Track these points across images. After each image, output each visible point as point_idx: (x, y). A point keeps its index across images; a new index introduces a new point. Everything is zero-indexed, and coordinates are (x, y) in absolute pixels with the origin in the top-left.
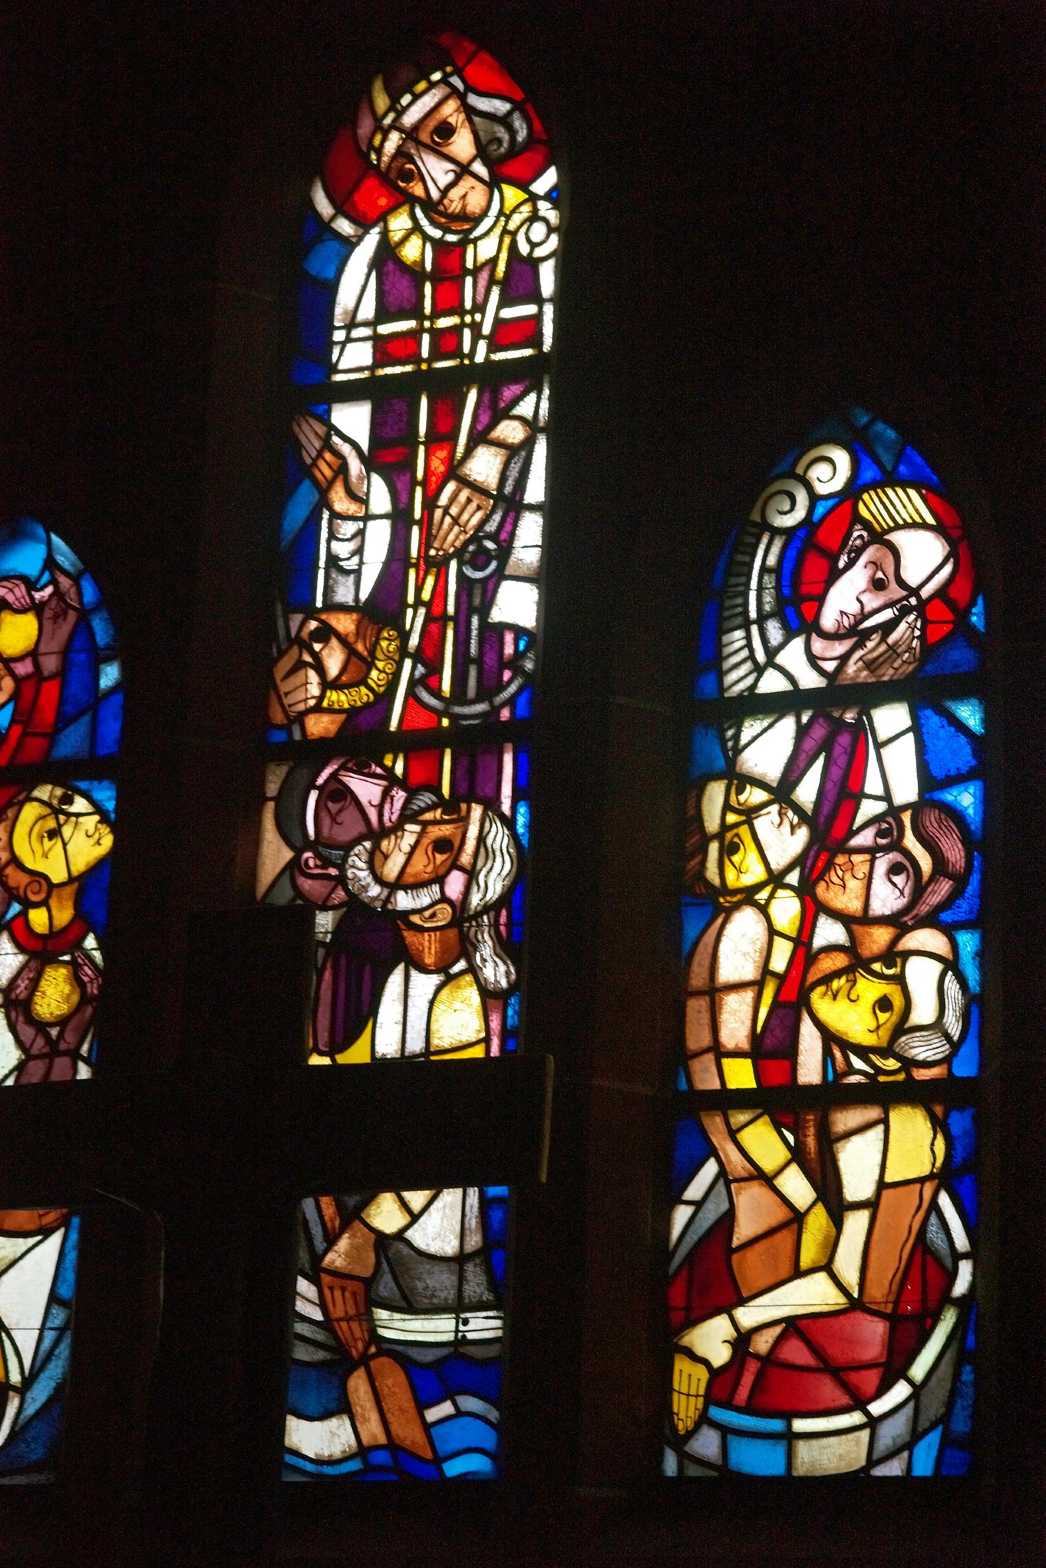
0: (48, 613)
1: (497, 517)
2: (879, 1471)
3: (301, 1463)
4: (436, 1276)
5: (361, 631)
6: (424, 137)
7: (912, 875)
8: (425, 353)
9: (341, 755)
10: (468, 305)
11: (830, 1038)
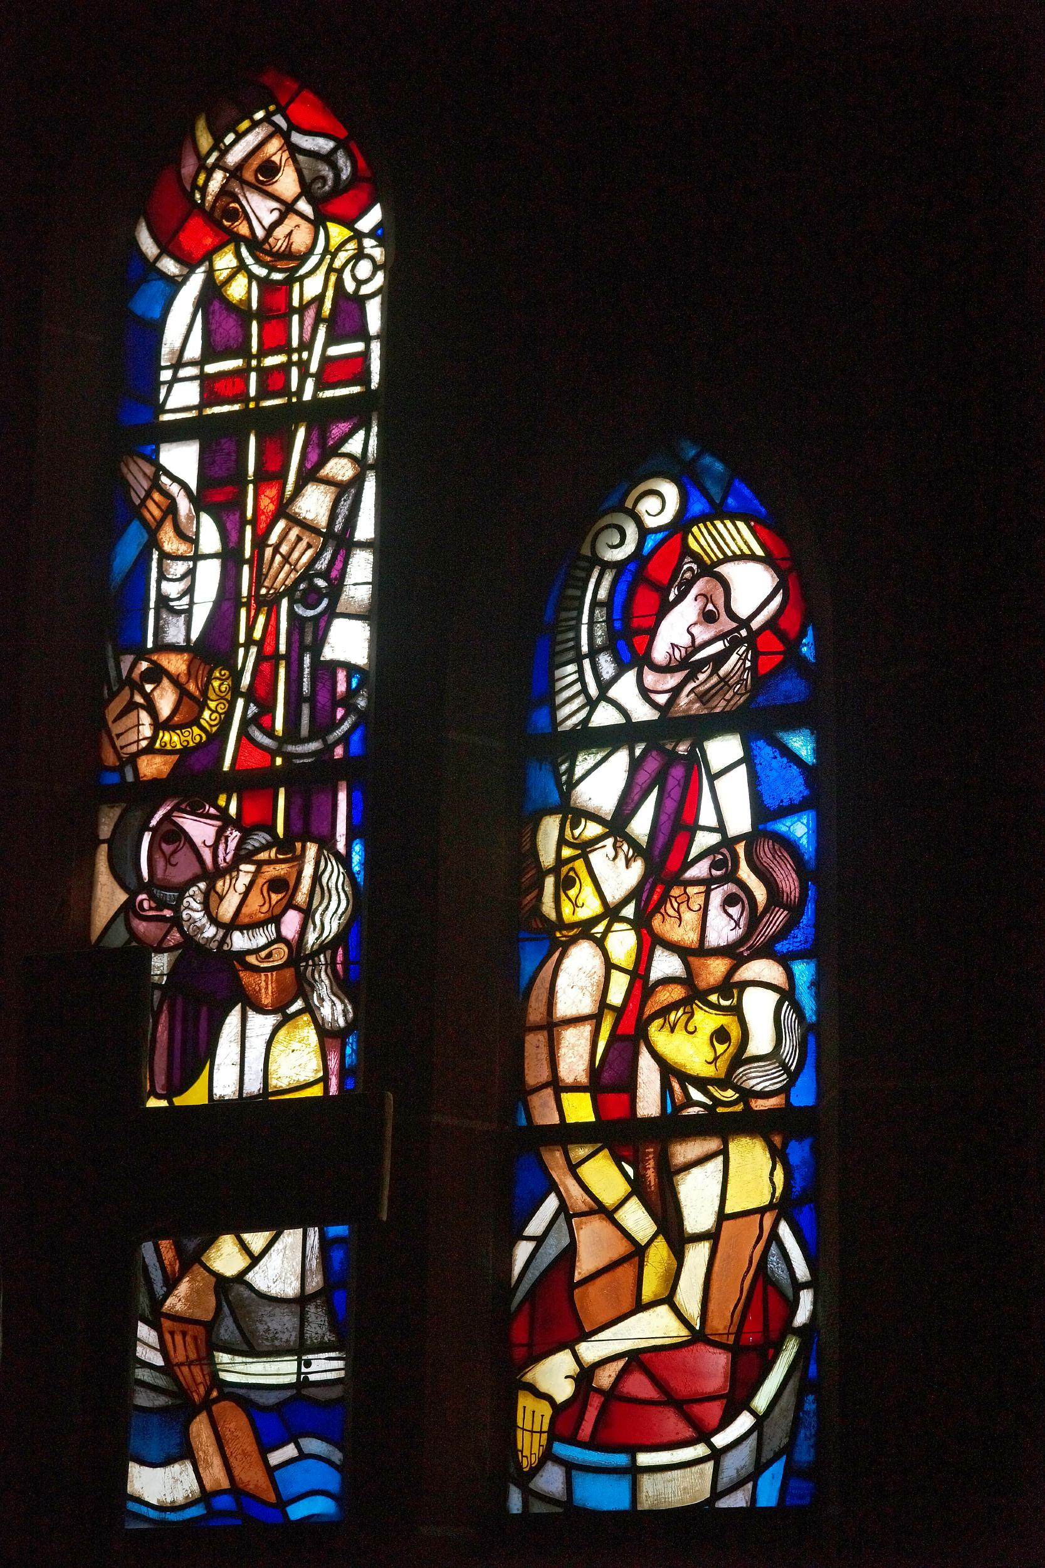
1: (328, 555)
2: (724, 1503)
3: (144, 1510)
5: (193, 672)
6: (248, 175)
7: (747, 906)
8: (252, 392)
9: (174, 796)
10: (295, 343)
11: (668, 1070)
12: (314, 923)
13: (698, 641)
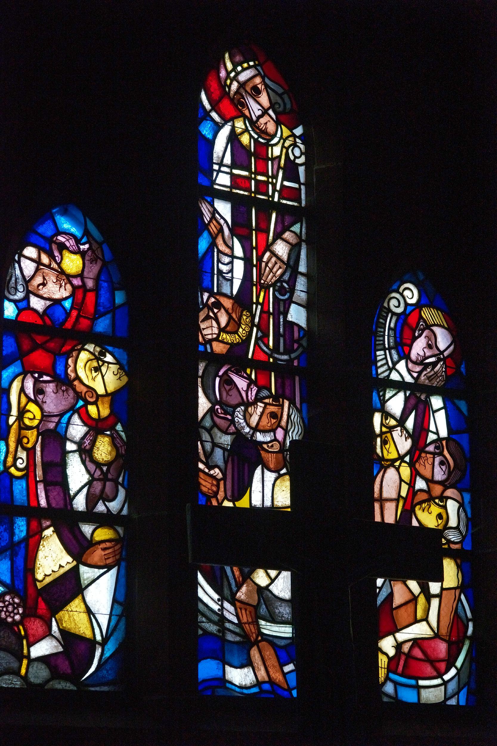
0: (87, 258)
2: (449, 703)
3: (233, 687)
4: (283, 608)
6: (248, 89)
10: (270, 174)
12: (289, 436)
13: (427, 355)
